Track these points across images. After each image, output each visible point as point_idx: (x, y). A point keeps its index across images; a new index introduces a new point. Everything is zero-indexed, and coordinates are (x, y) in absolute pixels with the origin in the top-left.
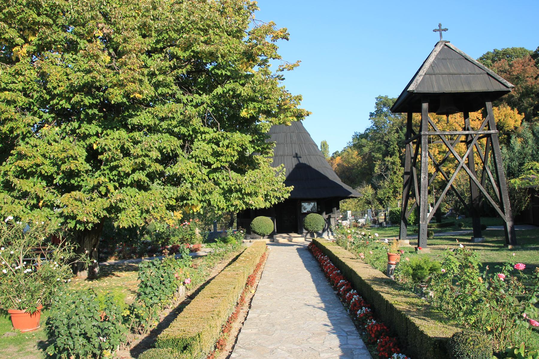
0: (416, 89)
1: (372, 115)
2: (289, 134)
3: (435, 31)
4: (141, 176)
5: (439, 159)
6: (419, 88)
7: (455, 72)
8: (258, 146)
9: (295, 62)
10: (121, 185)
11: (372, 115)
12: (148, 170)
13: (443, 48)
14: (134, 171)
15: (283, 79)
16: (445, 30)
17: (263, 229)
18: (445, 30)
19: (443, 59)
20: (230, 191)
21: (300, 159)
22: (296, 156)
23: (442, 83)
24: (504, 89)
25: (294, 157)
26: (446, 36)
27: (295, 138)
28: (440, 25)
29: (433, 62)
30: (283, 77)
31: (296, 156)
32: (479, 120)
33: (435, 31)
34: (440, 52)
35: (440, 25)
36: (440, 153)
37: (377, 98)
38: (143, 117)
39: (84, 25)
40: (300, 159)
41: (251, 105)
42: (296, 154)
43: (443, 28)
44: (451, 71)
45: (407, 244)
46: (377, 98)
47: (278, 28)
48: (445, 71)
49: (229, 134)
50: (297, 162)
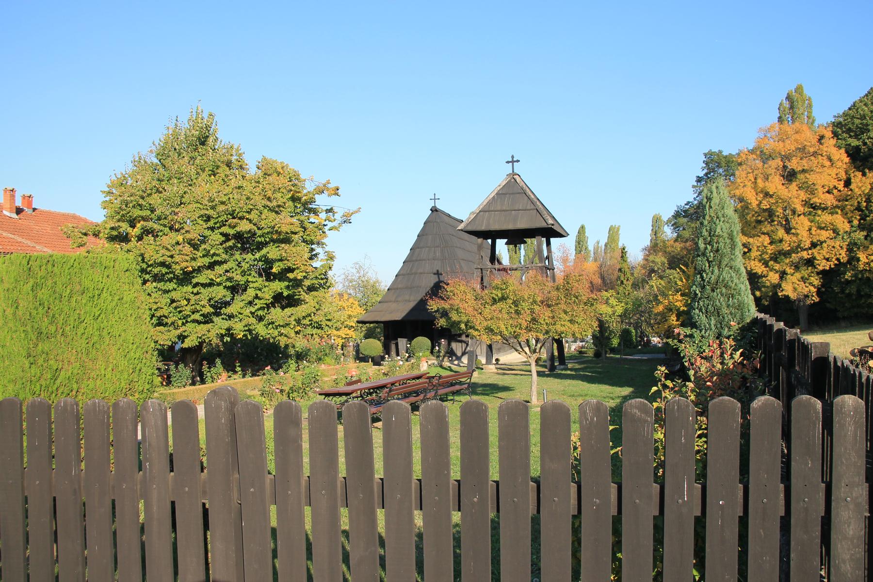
1: (699, 179)
3: (508, 162)
4: (197, 316)
5: (770, 252)
9: (355, 209)
10: (187, 322)
11: (699, 179)
12: (201, 313)
13: (510, 181)
14: (193, 313)
16: (518, 161)
18: (518, 161)
20: (269, 324)
22: (438, 273)
24: (544, 225)
27: (438, 254)
28: (513, 157)
31: (438, 273)
32: (840, 191)
33: (508, 162)
35: (513, 157)
36: (771, 243)
37: (705, 155)
38: (202, 278)
39: (165, 218)
41: (277, 264)
46: (705, 155)
47: (332, 186)
48: (499, 208)
49: (267, 284)
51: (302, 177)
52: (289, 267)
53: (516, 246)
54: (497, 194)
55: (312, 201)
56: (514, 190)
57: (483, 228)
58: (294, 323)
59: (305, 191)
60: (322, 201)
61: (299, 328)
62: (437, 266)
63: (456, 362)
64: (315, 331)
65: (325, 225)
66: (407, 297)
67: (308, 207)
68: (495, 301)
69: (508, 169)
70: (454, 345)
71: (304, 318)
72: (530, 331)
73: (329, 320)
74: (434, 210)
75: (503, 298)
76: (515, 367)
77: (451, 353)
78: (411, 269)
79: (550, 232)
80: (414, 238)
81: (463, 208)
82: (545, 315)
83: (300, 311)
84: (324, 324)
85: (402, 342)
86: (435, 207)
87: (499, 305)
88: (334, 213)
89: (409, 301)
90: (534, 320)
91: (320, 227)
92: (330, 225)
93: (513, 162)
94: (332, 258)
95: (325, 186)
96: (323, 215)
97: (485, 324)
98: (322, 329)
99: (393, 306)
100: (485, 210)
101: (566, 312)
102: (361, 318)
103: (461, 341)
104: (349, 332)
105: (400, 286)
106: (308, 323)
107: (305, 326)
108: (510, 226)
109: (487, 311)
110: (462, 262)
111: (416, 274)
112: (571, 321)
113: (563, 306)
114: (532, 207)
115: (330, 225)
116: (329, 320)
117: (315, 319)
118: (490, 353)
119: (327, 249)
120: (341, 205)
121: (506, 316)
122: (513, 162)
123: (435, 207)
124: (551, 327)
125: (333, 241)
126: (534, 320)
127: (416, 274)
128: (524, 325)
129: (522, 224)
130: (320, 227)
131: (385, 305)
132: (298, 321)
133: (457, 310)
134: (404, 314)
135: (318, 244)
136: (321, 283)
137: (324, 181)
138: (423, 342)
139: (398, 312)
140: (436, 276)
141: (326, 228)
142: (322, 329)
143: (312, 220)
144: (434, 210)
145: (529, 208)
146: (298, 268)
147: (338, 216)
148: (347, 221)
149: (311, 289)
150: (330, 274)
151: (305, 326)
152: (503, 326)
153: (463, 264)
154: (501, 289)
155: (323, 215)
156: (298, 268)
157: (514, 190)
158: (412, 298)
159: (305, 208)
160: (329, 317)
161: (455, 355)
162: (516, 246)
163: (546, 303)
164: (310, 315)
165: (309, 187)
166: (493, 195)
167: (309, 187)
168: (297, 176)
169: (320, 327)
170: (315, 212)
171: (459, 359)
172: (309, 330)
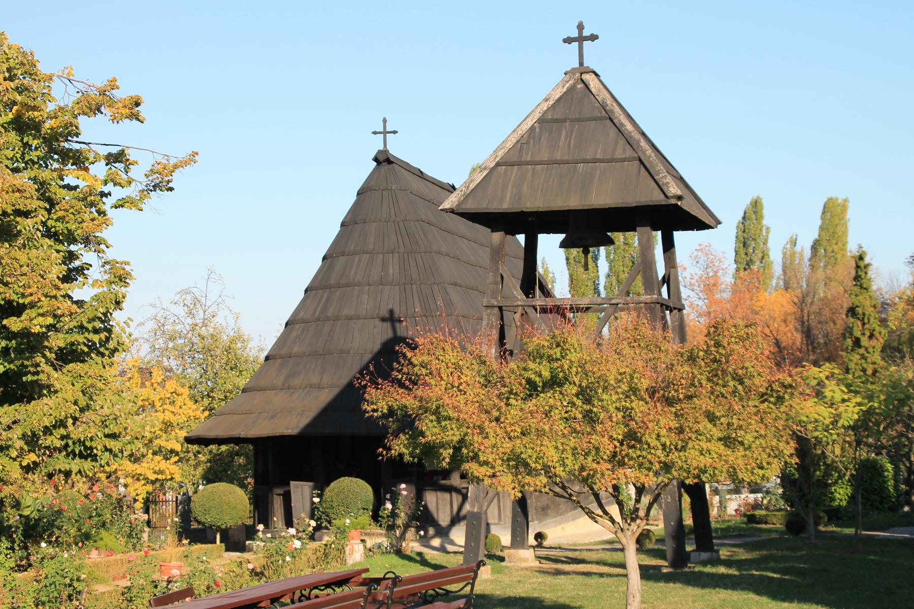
0: (459, 204)
2: (380, 257)
3: (568, 40)
6: (470, 201)
7: (566, 158)
8: (9, 363)
13: (572, 89)
15: (171, 189)
16: (593, 38)
17: (214, 513)
18: (593, 38)
19: (557, 121)
21: (397, 325)
23: (525, 188)
24: (656, 198)
25: (383, 320)
26: (593, 55)
27: (393, 270)
28: (580, 27)
29: (532, 128)
30: (170, 185)
31: (391, 319)
33: (568, 40)
34: (559, 100)
35: (580, 27)
40: (397, 325)
42: (391, 312)
43: (586, 33)
44: (558, 156)
45: (526, 560)
48: (545, 156)
50: (390, 334)
51: (43, 68)
52: (9, 302)
53: (586, 252)
54: (541, 121)
55: (70, 131)
56: (582, 112)
57: (506, 205)
58: (20, 444)
59: (51, 107)
60: (96, 133)
61: (33, 457)
62: (390, 300)
63: (436, 542)
64: (75, 465)
65: (103, 195)
66: (314, 379)
67: (57, 145)
68: (533, 390)
69: (569, 57)
70: (431, 499)
71: (47, 431)
72: (622, 464)
73: (114, 436)
74: (384, 160)
75: (554, 383)
76: (586, 555)
77: (423, 519)
78: (325, 309)
79: (675, 216)
80: (333, 230)
81: (457, 153)
82: (659, 424)
83: (38, 413)
84: (98, 445)
85: (302, 492)
86: (385, 152)
87: (546, 399)
88: (128, 165)
89: (320, 387)
90: (632, 438)
91: (92, 200)
92: (118, 193)
93: (581, 39)
94: (122, 278)
95: (103, 93)
96: (99, 170)
97: (508, 446)
98: (94, 458)
99: (279, 399)
100: (511, 161)
101: (712, 418)
102: (196, 430)
103: (450, 489)
104: (164, 465)
105: (296, 350)
106: (58, 443)
107: (52, 451)
108: (574, 202)
109: (515, 410)
110: (451, 290)
111: (337, 318)
112: (727, 441)
113: (704, 403)
114: (629, 153)
115: (118, 193)
116: (114, 436)
117: (77, 432)
118: (521, 519)
119: (110, 254)
120: (145, 144)
121: (561, 426)
122: (581, 39)
123: (385, 152)
124: (674, 456)
125: (124, 234)
126: (632, 438)
127: (337, 318)
128: (608, 448)
129: (603, 195)
130: (92, 200)
131: (257, 398)
132: (32, 441)
133: (436, 412)
134: (305, 421)
135: (87, 241)
136: (95, 340)
137: (100, 81)
138: (354, 489)
139: (290, 414)
140: (388, 325)
141: (109, 202)
142: (94, 458)
143: (70, 180)
144: (384, 160)
145: (619, 155)
146: (32, 305)
147: (138, 173)
148: (161, 183)
149: (68, 356)
150: (118, 317)
151: (52, 451)
152: (552, 452)
153: (455, 295)
154: (551, 359)
155: (99, 170)
156: (32, 305)
157: (582, 112)
158: (326, 380)
159: (52, 150)
160: (113, 428)
161: (434, 523)
162: (586, 252)
163: (663, 395)
164: (62, 424)
165: (62, 96)
166: (530, 123)
167: (62, 96)
168: (29, 67)
169: (88, 454)
170: (79, 160)
171: (443, 532)
172: (61, 462)
